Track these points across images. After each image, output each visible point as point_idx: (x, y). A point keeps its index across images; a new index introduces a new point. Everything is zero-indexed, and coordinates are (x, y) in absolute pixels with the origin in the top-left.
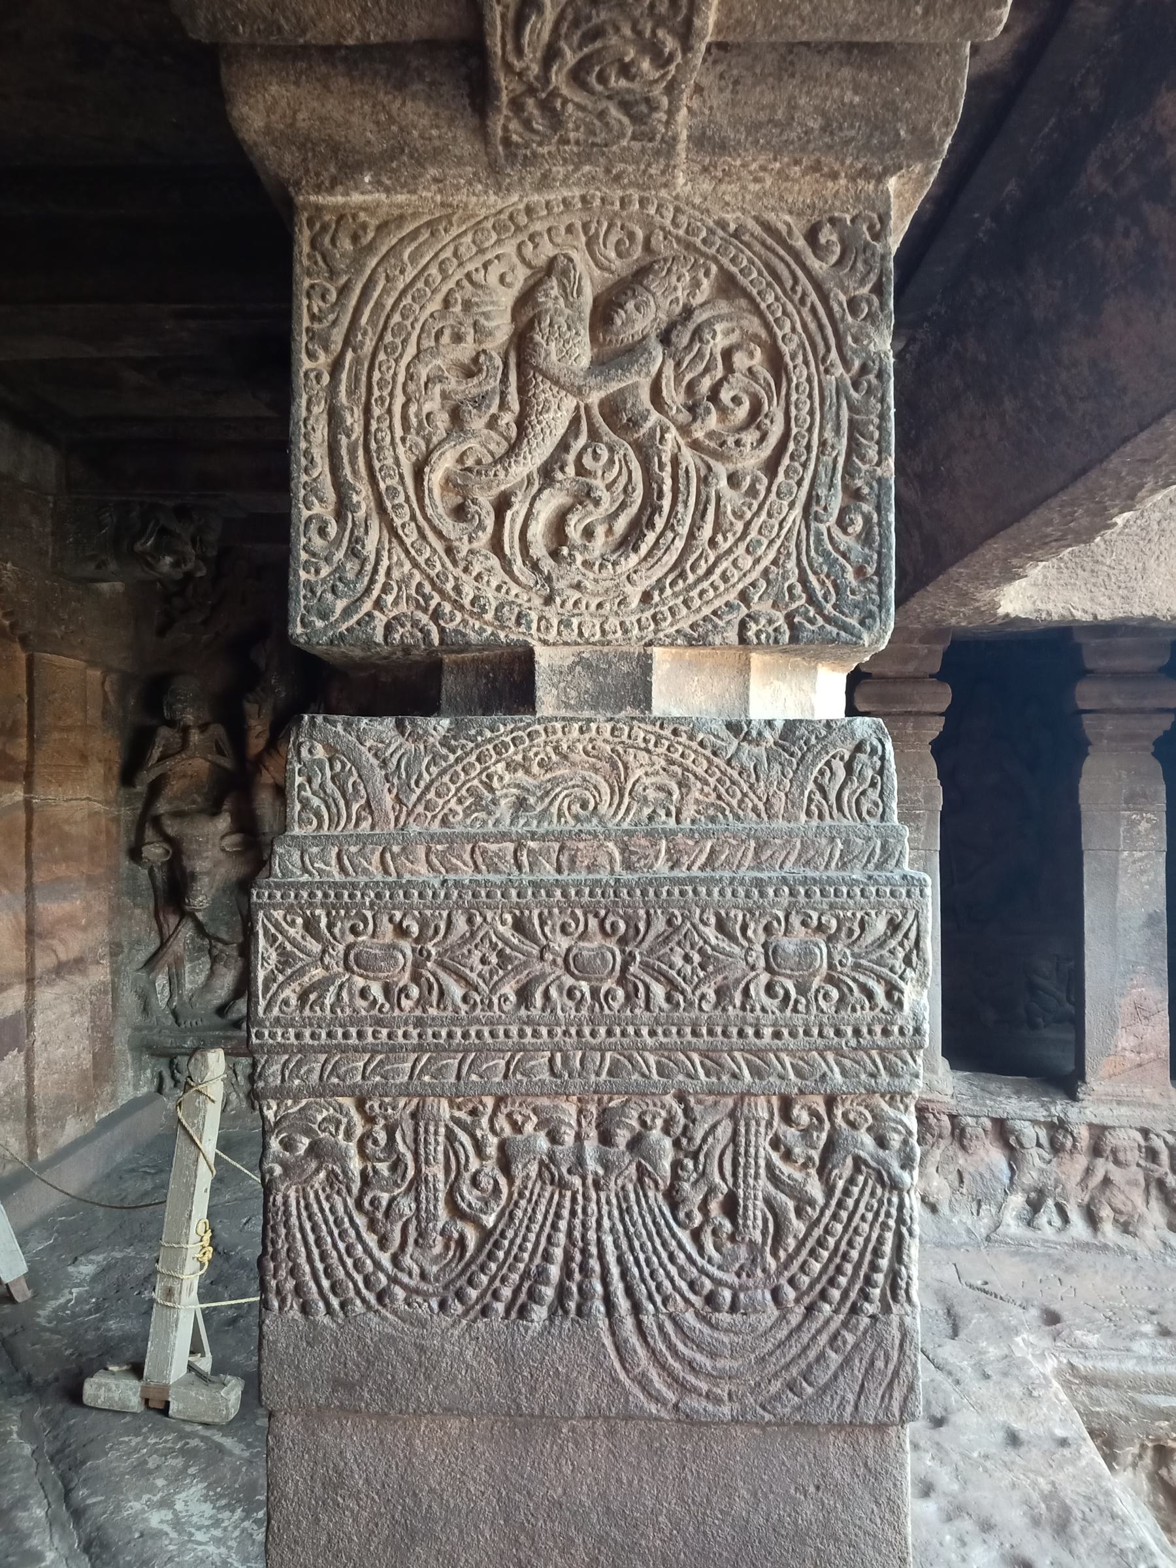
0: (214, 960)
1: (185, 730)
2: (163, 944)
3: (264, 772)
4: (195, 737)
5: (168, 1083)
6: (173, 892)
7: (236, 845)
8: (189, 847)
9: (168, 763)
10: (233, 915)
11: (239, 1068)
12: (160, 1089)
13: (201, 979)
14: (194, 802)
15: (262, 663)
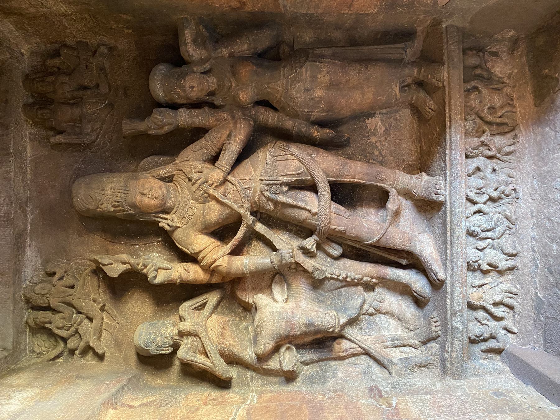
0: (378, 311)
1: (182, 334)
2: (367, 354)
3: (217, 263)
4: (186, 326)
5: (492, 344)
6: (320, 342)
7: (283, 290)
8: (282, 328)
9: (208, 348)
10: (340, 294)
11: (477, 283)
12: (499, 352)
13: (393, 322)
14: (246, 328)
15: (122, 268)
